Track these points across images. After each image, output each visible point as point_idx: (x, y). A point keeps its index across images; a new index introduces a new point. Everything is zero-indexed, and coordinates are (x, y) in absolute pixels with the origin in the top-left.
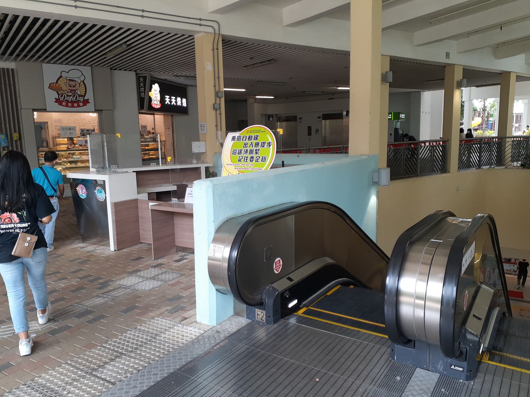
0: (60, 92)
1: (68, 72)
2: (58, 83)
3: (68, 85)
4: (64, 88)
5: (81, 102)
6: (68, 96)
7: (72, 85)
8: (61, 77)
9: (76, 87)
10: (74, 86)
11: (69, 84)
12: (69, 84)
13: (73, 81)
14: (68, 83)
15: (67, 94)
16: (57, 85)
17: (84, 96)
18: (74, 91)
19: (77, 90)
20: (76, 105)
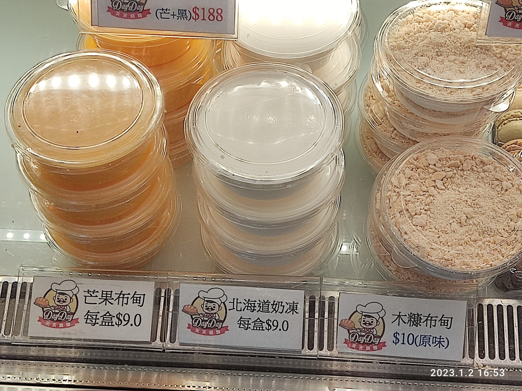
0: (351, 332)
1: (365, 306)
2: (351, 320)
3: (362, 322)
4: (358, 326)
5: (375, 345)
6: (360, 336)
7: (368, 322)
8: (356, 311)
9: (372, 325)
10: (370, 324)
11: (364, 321)
12: (364, 321)
13: (369, 317)
14: (362, 320)
15: (360, 333)
16: (350, 322)
17: (380, 337)
18: (369, 332)
19: (373, 328)
20: (368, 348)
